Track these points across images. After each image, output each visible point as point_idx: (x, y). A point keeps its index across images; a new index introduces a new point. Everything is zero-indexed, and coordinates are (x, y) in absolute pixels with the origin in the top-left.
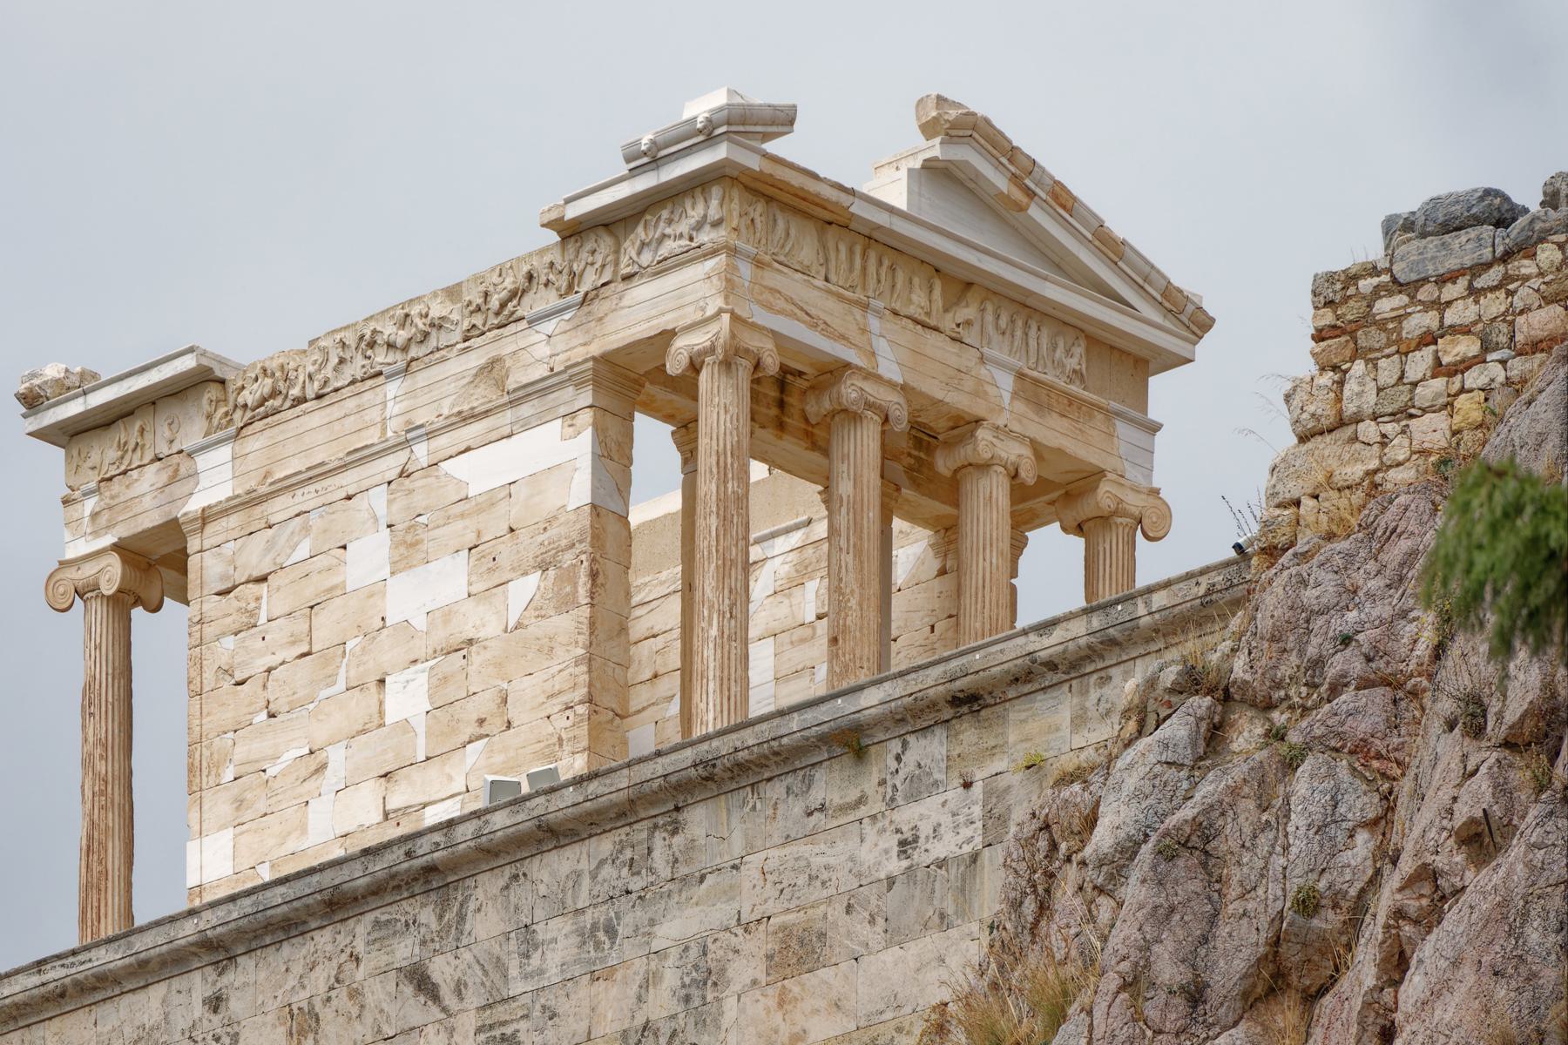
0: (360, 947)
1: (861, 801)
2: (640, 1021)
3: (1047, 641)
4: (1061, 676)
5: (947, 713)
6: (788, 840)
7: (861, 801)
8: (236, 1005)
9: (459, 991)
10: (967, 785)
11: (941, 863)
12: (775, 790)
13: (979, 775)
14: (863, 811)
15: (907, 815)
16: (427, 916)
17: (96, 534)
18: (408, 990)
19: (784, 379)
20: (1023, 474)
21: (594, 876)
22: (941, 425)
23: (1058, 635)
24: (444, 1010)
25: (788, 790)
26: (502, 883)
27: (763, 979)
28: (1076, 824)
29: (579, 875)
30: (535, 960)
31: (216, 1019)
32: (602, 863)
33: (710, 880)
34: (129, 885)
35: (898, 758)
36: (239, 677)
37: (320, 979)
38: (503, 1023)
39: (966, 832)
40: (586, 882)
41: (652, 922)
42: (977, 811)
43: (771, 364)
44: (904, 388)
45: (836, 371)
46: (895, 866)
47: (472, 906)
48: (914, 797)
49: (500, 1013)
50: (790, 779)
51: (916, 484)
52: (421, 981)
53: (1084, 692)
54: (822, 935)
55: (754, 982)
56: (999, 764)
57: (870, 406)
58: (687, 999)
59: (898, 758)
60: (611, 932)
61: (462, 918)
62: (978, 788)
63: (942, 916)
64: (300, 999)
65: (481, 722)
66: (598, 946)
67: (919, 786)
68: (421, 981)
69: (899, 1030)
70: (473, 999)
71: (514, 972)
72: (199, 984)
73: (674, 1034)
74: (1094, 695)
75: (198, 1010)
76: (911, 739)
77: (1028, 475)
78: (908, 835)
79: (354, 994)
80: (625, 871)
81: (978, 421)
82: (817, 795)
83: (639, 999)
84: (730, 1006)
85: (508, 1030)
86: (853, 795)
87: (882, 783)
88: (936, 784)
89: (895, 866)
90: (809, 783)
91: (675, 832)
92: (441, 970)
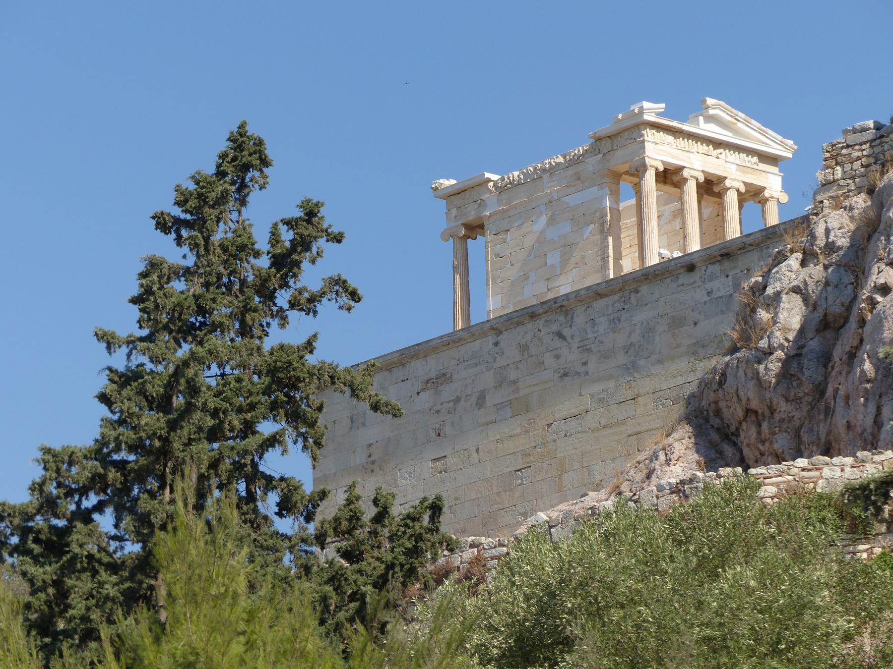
0: (541, 328)
1: (695, 282)
2: (629, 343)
3: (749, 239)
4: (754, 247)
5: (720, 258)
6: (673, 293)
7: (695, 282)
8: (502, 344)
9: (572, 337)
10: (727, 276)
11: (720, 297)
12: (668, 280)
13: (731, 274)
14: (695, 285)
15: (709, 286)
16: (562, 318)
17: (456, 221)
18: (556, 338)
19: (666, 171)
20: (741, 190)
21: (613, 306)
23: (752, 237)
24: (568, 343)
25: (672, 281)
26: (584, 308)
27: (667, 329)
28: (761, 288)
29: (608, 306)
30: (596, 328)
31: (496, 348)
32: (615, 302)
33: (649, 305)
34: (469, 311)
35: (705, 271)
36: (501, 256)
37: (529, 337)
38: (587, 345)
39: (727, 289)
40: (610, 308)
41: (632, 316)
42: (731, 283)
43: (661, 169)
44: (703, 171)
45: (681, 169)
46: (706, 299)
47: (575, 315)
48: (711, 280)
49: (586, 342)
50: (672, 278)
52: (560, 336)
53: (762, 251)
54: (685, 318)
55: (664, 331)
56: (738, 271)
57: (691, 176)
58: (644, 336)
59: (705, 271)
60: (619, 320)
61: (572, 318)
62: (730, 278)
63: (722, 311)
65: (577, 264)
66: (615, 324)
67: (712, 278)
68: (560, 336)
69: (710, 341)
70: (577, 339)
71: (589, 331)
72: (491, 339)
74: (765, 252)
75: (491, 346)
76: (709, 266)
77: (743, 189)
78: (710, 290)
79: (540, 340)
80: (622, 304)
81: (726, 178)
82: (680, 281)
83: (629, 337)
85: (588, 347)
86: (692, 281)
87: (701, 277)
88: (718, 277)
89: (706, 299)
90: (677, 278)
91: (637, 293)
92: (566, 332)
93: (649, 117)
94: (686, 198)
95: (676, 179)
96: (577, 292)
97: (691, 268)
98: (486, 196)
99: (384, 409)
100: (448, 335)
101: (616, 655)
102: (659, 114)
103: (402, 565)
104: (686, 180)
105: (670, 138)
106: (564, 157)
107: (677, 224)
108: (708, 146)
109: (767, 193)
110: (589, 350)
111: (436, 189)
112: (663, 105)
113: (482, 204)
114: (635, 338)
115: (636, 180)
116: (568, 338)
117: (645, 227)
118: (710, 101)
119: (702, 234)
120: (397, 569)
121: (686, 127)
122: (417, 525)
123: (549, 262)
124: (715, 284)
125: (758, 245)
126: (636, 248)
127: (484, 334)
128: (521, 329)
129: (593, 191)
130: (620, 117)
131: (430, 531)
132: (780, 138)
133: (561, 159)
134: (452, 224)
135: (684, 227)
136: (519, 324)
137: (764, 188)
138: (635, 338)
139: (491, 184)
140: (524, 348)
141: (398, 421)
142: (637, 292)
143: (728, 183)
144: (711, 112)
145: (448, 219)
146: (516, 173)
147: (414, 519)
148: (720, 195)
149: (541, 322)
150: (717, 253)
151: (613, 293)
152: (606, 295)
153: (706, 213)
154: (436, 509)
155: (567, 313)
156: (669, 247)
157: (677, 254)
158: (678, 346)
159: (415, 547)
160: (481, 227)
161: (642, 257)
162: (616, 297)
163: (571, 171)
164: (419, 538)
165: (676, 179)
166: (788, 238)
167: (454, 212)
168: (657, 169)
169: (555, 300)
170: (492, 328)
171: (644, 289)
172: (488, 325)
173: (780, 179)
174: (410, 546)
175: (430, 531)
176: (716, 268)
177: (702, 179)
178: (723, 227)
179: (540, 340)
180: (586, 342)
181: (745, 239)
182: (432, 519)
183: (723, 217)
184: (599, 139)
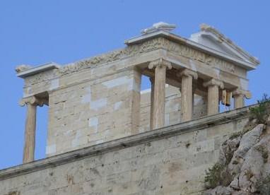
0: (83, 165)
9: (103, 172)
18: (92, 173)
44: (198, 72)
49: (112, 177)
51: (199, 88)
52: (96, 171)
68: (96, 171)
73: (149, 181)
79: (81, 173)
81: (212, 78)
92: (100, 169)
108: (202, 55)
114: (147, 175)
116: (100, 173)
148: (206, 89)
158: (175, 183)
168: (167, 67)
177: (196, 77)
180: (112, 177)
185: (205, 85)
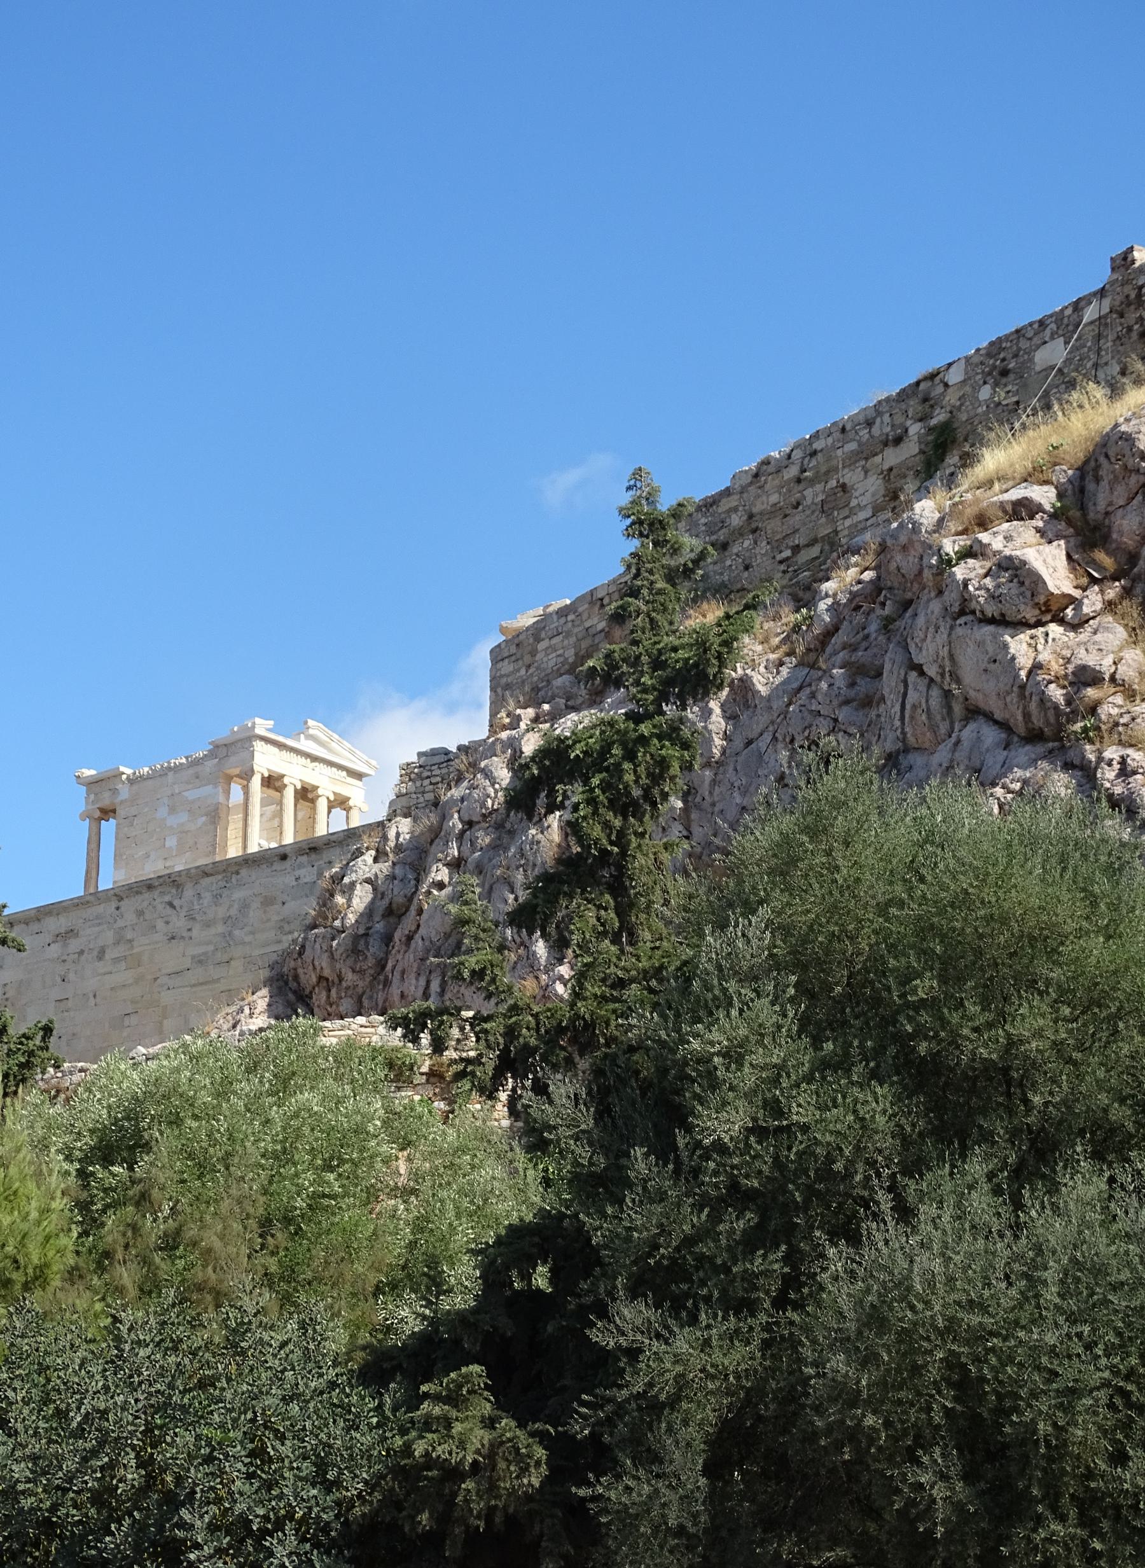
8: (122, 909)
13: (316, 864)
15: (297, 873)
16: (174, 891)
19: (270, 777)
22: (309, 788)
37: (145, 904)
43: (266, 775)
45: (283, 776)
46: (294, 883)
52: (171, 905)
56: (321, 862)
64: (139, 908)
67: (301, 866)
68: (171, 905)
75: (113, 909)
77: (332, 798)
82: (274, 868)
84: (251, 913)
92: (176, 903)
93: (259, 731)
94: (285, 801)
95: (278, 784)
96: (188, 870)
97: (284, 857)
98: (120, 786)
99: (11, 944)
100: (78, 898)
101: (187, 1159)
102: (269, 730)
103: (15, 1077)
104: (286, 786)
105: (275, 750)
106: (187, 758)
107: (276, 822)
109: (351, 803)
110: (194, 919)
111: (79, 777)
112: (272, 722)
113: (115, 791)
114: (233, 912)
115: (245, 783)
117: (249, 822)
118: (311, 723)
119: (296, 832)
120: (11, 1078)
121: (290, 742)
122: (31, 1043)
123: (168, 844)
124: (302, 872)
125: (340, 842)
126: (240, 840)
127: (108, 900)
128: (139, 898)
129: (208, 789)
130: (236, 729)
131: (42, 1048)
132: (366, 758)
133: (184, 761)
134: (90, 807)
135: (281, 826)
136: (138, 893)
137: (349, 799)
138: (233, 912)
139: (124, 777)
140: (140, 913)
141: (23, 954)
142: (238, 873)
143: (320, 792)
144: (311, 731)
145: (87, 803)
146: (146, 769)
147: (28, 1038)
148: (313, 801)
149: (156, 893)
150: (306, 847)
151: (218, 873)
152: (212, 875)
153: (300, 815)
154: (48, 1030)
155: (178, 886)
156: (269, 840)
157: (274, 845)
158: (269, 920)
159: (28, 1062)
160: (114, 811)
161: (245, 847)
162: (220, 877)
163: (191, 771)
164: (31, 1054)
165: (278, 784)
166: (365, 838)
167: (92, 797)
169: (169, 876)
170: (116, 895)
171: (244, 872)
172: (112, 892)
173: (363, 792)
174: (23, 1060)
175: (42, 1048)
176: (304, 859)
177: (299, 787)
178: (313, 827)
179: (154, 907)
181: (331, 837)
182: (43, 1039)
183: (314, 819)
184: (217, 747)
185: (310, 796)
